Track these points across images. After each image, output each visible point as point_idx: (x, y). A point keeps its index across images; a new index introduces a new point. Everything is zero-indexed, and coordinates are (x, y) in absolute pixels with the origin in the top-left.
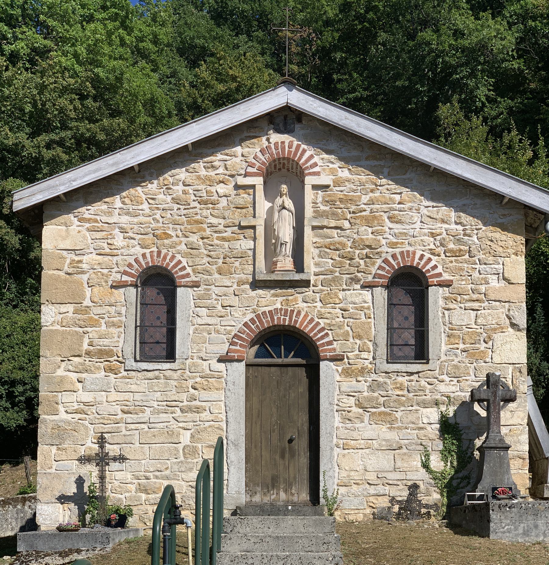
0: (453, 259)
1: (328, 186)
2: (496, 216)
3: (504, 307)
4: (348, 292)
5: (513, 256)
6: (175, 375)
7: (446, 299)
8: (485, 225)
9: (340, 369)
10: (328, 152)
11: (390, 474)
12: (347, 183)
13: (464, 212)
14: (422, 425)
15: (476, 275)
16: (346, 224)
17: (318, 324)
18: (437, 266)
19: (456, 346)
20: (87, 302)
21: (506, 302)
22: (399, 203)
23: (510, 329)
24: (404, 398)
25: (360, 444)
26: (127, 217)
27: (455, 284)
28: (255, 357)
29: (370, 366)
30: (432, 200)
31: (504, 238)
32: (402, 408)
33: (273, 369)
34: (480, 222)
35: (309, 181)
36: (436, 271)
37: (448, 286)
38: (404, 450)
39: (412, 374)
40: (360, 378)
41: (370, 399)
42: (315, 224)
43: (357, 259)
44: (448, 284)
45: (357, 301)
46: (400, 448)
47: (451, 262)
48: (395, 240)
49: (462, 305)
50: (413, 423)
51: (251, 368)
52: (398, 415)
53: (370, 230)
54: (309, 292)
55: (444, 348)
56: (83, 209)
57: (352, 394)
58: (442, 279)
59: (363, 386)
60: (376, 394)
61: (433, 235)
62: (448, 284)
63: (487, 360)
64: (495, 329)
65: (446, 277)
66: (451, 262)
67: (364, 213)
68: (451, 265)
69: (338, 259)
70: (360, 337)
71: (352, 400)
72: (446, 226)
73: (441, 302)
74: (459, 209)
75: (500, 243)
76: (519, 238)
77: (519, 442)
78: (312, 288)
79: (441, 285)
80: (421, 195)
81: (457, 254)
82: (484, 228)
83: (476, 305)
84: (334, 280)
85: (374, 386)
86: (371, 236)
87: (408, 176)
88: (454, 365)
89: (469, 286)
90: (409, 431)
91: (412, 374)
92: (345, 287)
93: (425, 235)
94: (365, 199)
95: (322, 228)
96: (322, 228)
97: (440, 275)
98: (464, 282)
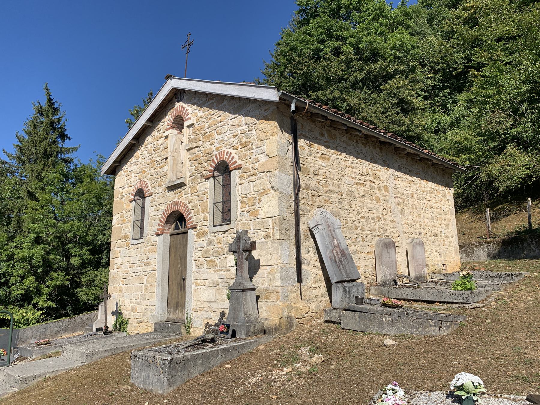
0: (243, 149)
1: (193, 124)
2: (263, 111)
3: (267, 175)
4: (200, 184)
5: (271, 137)
6: (142, 245)
7: (240, 177)
8: (258, 120)
9: (196, 233)
10: (194, 104)
11: (213, 303)
12: (201, 119)
13: (247, 115)
14: (228, 268)
15: (253, 157)
16: (200, 143)
17: (188, 206)
18: (235, 157)
19: (244, 209)
20: (124, 212)
21: (268, 172)
22: (221, 122)
23: (272, 191)
24: (220, 250)
25: (201, 283)
26: (135, 166)
27: (243, 166)
28: (175, 230)
29: (207, 229)
30: (234, 114)
31: (266, 126)
32: (220, 257)
33: (179, 236)
34: (255, 119)
35: (186, 124)
36: (234, 160)
37: (240, 168)
38: (220, 287)
39: (225, 232)
40: (203, 238)
41: (206, 252)
42: (187, 148)
43: (204, 163)
44: (239, 168)
45: (203, 189)
46: (218, 285)
47: (242, 151)
48: (219, 146)
49: (247, 180)
50: (224, 266)
51: (172, 237)
52: (218, 262)
53: (209, 143)
54: (187, 189)
55: (239, 210)
56: (124, 167)
57: (200, 249)
58: (236, 164)
59: (205, 244)
60: (209, 248)
61: (235, 136)
62: (239, 168)
63: (259, 216)
64: (262, 193)
65: (239, 162)
66: (242, 151)
67: (207, 134)
68: (242, 153)
69: (197, 165)
70: (203, 212)
71: (200, 253)
72: (241, 128)
73: (238, 180)
74: (245, 115)
75: (265, 131)
76: (273, 122)
77: (275, 279)
78: (188, 186)
79: (236, 169)
80: (229, 113)
81: (245, 145)
82: (258, 122)
83: (252, 178)
84: (195, 179)
85: (210, 242)
86: (209, 146)
87: (224, 103)
88: (243, 223)
89: (250, 166)
90: (222, 272)
91: (225, 232)
92: (199, 181)
93: (231, 138)
94: (207, 125)
95: (191, 149)
96: (191, 149)
97: (235, 162)
98: (248, 164)
